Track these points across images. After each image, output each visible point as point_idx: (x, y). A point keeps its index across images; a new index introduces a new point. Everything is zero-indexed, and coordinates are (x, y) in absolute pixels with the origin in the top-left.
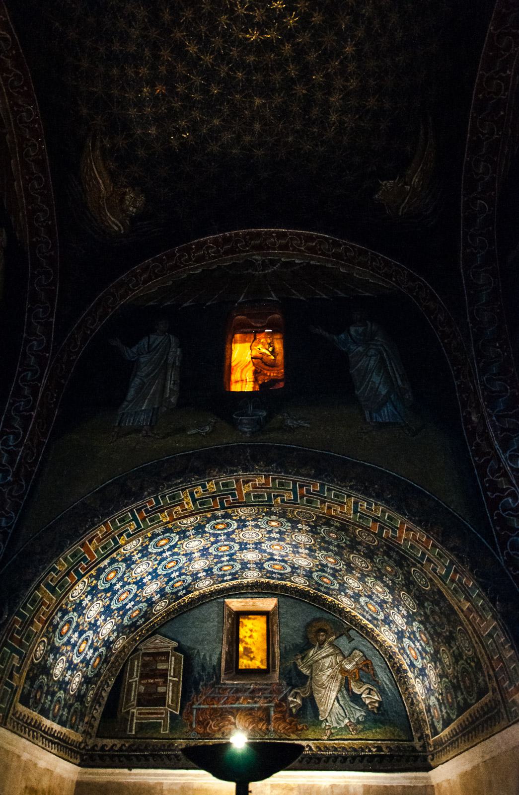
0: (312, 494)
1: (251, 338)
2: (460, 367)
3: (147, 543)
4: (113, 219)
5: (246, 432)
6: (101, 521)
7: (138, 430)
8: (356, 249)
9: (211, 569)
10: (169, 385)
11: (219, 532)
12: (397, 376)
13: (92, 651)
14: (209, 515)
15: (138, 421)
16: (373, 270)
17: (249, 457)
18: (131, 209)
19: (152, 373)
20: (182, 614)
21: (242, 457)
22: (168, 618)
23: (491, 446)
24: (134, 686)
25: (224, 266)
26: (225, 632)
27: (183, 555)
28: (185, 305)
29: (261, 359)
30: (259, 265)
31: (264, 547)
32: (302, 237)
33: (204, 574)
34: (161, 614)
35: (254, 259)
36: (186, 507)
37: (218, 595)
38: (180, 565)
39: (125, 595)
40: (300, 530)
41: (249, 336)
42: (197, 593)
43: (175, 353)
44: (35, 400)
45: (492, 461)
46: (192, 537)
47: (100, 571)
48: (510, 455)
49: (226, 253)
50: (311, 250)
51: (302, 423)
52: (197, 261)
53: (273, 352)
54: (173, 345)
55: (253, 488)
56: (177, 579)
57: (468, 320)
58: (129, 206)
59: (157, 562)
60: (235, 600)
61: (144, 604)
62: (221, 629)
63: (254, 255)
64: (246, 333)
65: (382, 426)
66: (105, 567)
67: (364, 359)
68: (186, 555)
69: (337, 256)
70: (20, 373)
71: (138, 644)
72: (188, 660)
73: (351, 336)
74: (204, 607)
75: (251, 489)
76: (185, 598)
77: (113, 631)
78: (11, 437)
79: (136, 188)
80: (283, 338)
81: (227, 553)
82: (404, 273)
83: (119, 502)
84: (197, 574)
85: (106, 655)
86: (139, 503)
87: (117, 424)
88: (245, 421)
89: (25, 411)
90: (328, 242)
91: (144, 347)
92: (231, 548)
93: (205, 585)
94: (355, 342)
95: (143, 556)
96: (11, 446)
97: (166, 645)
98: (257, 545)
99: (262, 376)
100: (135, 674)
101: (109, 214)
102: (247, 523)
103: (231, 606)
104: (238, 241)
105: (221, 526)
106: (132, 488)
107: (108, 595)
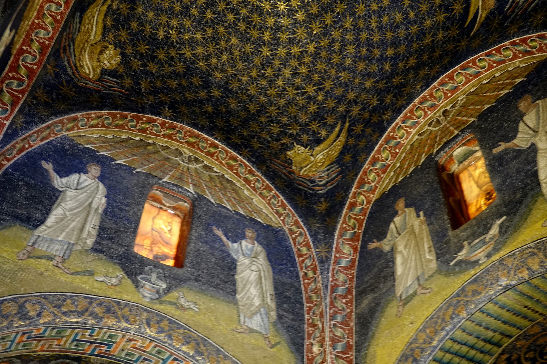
4: (88, 63)
7: (50, 258)
17: (144, 321)
18: (106, 62)
21: (138, 318)
28: (118, 162)
32: (229, 155)
43: (100, 200)
49: (164, 136)
50: (231, 167)
51: (192, 305)
52: (139, 130)
54: (100, 192)
57: (330, 274)
63: (184, 147)
67: (248, 271)
69: (248, 181)
73: (242, 248)
79: (117, 49)
83: (12, 321)
87: (30, 244)
88: (148, 287)
90: (246, 168)
94: (243, 254)
99: (157, 248)
101: (87, 57)
104: (179, 132)
106: (28, 312)
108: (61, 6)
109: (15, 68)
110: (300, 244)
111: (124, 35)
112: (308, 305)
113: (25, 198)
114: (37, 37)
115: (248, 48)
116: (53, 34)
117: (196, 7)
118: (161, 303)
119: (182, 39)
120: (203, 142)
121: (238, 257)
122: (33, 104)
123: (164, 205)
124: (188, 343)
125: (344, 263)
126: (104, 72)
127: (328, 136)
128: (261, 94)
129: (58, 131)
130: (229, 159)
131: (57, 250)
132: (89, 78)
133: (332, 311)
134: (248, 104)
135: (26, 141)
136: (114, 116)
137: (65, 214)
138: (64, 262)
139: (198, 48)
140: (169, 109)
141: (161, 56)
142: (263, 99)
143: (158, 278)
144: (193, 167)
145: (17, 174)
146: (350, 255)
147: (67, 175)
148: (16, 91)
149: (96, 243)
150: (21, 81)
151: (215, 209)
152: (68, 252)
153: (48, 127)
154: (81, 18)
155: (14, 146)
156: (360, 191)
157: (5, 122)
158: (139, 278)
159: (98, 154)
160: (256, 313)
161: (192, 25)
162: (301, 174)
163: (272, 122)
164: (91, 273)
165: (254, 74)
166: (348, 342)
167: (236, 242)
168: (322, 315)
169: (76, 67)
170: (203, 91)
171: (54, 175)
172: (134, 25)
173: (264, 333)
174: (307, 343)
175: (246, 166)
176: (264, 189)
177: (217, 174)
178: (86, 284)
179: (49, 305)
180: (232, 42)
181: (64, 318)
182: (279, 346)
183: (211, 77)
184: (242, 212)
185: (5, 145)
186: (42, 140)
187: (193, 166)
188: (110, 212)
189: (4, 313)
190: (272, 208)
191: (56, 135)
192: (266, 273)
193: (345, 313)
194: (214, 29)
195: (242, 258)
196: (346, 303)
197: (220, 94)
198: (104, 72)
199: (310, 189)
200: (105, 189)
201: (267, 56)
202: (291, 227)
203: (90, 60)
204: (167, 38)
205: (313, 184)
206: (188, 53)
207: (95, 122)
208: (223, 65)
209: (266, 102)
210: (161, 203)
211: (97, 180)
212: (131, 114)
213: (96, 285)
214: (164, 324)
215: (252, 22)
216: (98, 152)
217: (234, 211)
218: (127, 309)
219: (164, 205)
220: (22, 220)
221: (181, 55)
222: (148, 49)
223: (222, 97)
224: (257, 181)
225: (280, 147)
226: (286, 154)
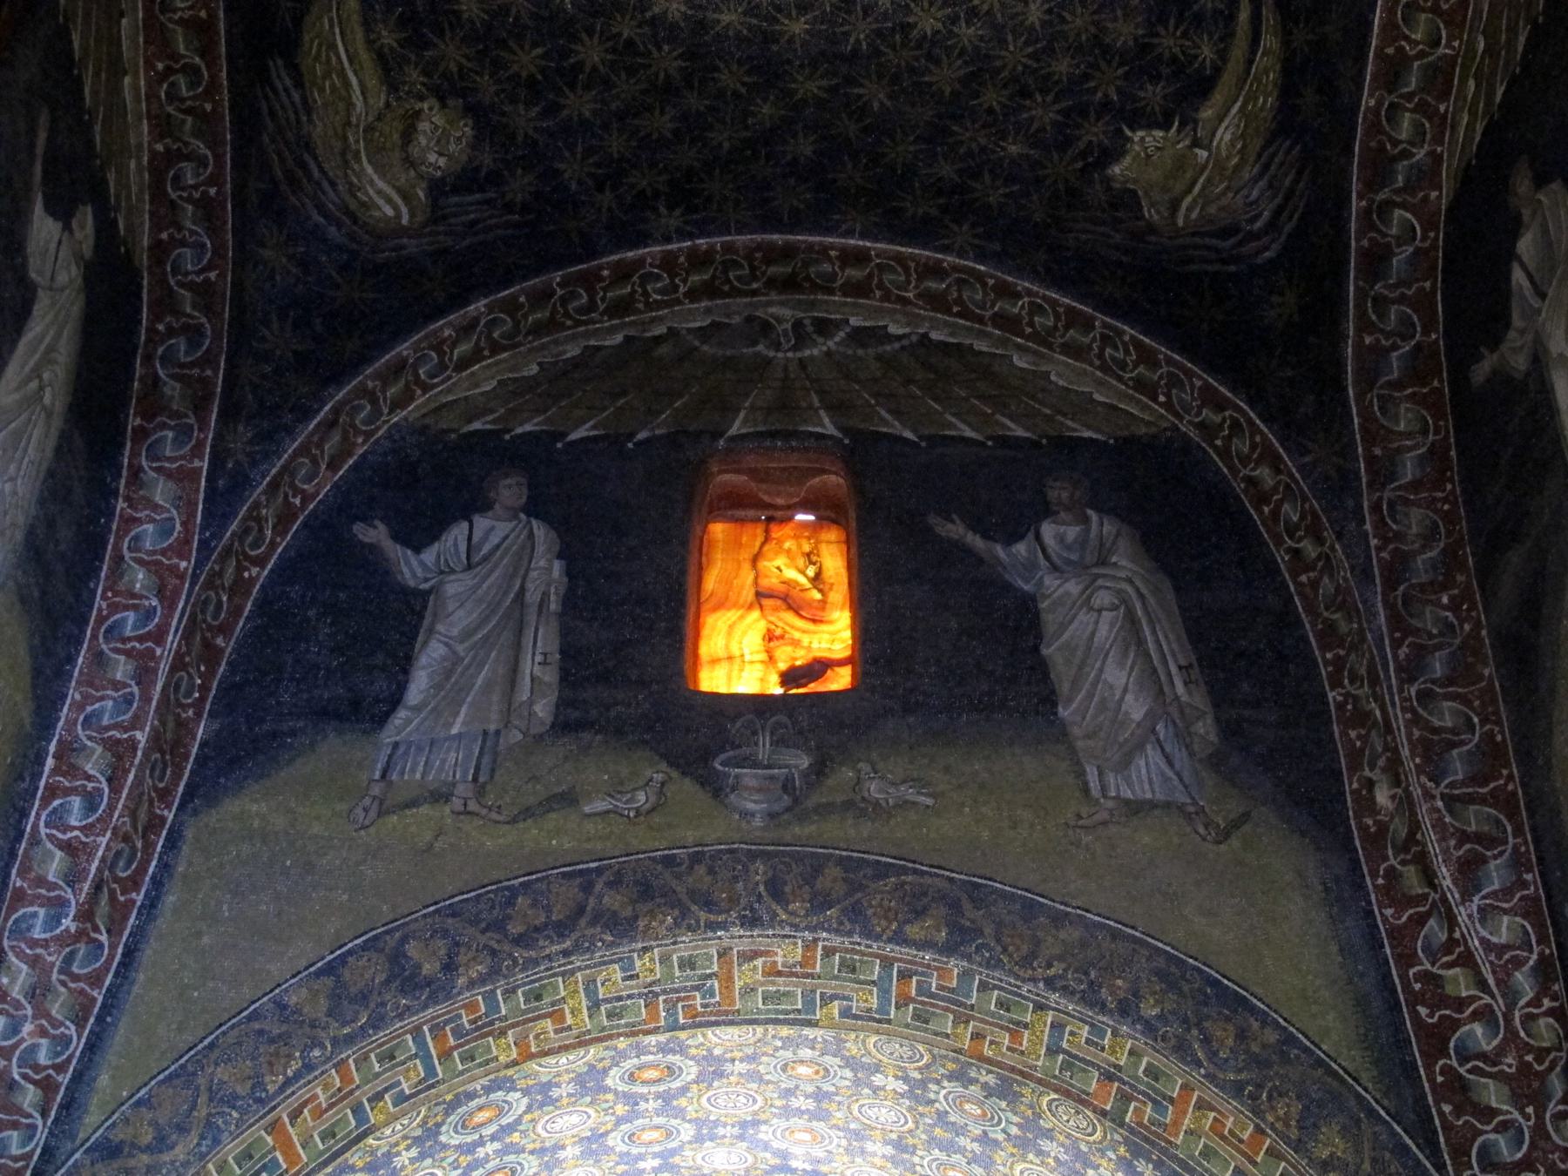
0: (932, 996)
1: (755, 536)
2: (1342, 653)
3: (439, 1119)
4: (381, 184)
5: (753, 815)
6: (329, 1059)
7: (440, 796)
8: (1061, 310)
10: (529, 666)
11: (645, 1090)
12: (1174, 670)
14: (622, 1043)
15: (441, 768)
16: (1104, 368)
17: (762, 888)
18: (432, 158)
21: (740, 885)
23: (1430, 878)
25: (689, 330)
27: (532, 1152)
28: (573, 436)
30: (785, 331)
31: (764, 1133)
35: (772, 315)
36: (569, 1021)
40: (876, 1090)
43: (547, 573)
44: (146, 699)
45: (1432, 922)
46: (565, 1101)
48: (1481, 910)
49: (693, 295)
50: (938, 302)
51: (910, 793)
53: (817, 579)
54: (540, 549)
55: (765, 974)
57: (1368, 527)
63: (769, 304)
64: (740, 521)
65: (1135, 809)
67: (1082, 616)
75: (759, 977)
78: (76, 802)
80: (848, 542)
81: (657, 1149)
82: (1192, 386)
83: (383, 1004)
86: (441, 1009)
87: (377, 775)
88: (753, 783)
90: (984, 285)
91: (457, 550)
92: (669, 1135)
94: (1055, 568)
95: (422, 1156)
96: (75, 828)
98: (747, 1127)
99: (789, 649)
101: (370, 170)
102: (728, 1067)
104: (728, 265)
105: (652, 1074)
106: (419, 966)
108: (196, 71)
109: (165, 303)
110: (1245, 461)
111: (453, 53)
112: (1329, 656)
114: (183, 189)
116: (219, 158)
118: (803, 818)
120: (817, 261)
121: (1040, 582)
122: (264, 377)
124: (920, 914)
125: (1409, 470)
126: (437, 188)
127: (1223, 55)
128: (954, 20)
131: (452, 764)
132: (403, 227)
133: (1403, 652)
136: (511, 306)
137: (454, 653)
140: (671, 208)
141: (592, 54)
142: (967, 33)
143: (779, 742)
144: (815, 352)
145: (295, 591)
146: (1425, 432)
147: (435, 538)
148: (192, 365)
149: (562, 704)
152: (486, 760)
153: (330, 424)
155: (255, 517)
156: (1381, 196)
157: (197, 463)
159: (507, 437)
160: (1141, 747)
162: (1180, 222)
163: (1025, 93)
164: (568, 799)
166: (1490, 736)
167: (1022, 537)
168: (1374, 681)
170: (765, 100)
171: (395, 552)
173: (1182, 798)
174: (1351, 785)
175: (980, 277)
176: (1067, 328)
177: (905, 342)
178: (558, 837)
179: (471, 930)
182: (1247, 828)
183: (777, 41)
184: (1020, 432)
185: (223, 527)
186: (333, 466)
188: (581, 601)
189: (353, 990)
190: (1120, 379)
192: (1152, 600)
193: (1458, 641)
195: (1050, 582)
196: (1454, 606)
197: (824, 83)
198: (437, 188)
199: (1224, 262)
200: (553, 534)
202: (1198, 414)
203: (383, 176)
205: (1232, 241)
207: (464, 348)
209: (981, 38)
211: (523, 516)
212: (558, 276)
213: (589, 827)
214: (831, 877)
216: (509, 431)
217: (989, 438)
218: (701, 870)
220: (339, 717)
222: (544, 56)
223: (832, 90)
224: (1036, 309)
225: (1080, 165)
226: (1107, 181)
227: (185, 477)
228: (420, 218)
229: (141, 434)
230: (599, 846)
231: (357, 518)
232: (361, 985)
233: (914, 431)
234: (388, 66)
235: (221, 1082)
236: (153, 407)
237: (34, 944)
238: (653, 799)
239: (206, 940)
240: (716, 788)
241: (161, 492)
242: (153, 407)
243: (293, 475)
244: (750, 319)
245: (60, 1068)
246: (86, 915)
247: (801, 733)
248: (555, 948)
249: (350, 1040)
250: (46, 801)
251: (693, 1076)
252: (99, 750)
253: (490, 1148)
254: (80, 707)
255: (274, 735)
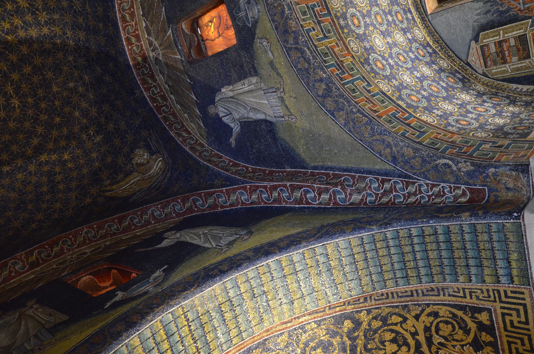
3: (381, 76)
4: (155, 167)
5: (258, 9)
7: (282, 99)
9: (403, 29)
13: (486, 104)
18: (145, 157)
19: (243, 106)
20: (447, 46)
21: (276, 5)
22: (453, 57)
24: (514, 67)
26: (454, 5)
27: (391, 50)
29: (218, 28)
33: (408, 34)
34: (451, 62)
37: (426, 21)
38: (401, 52)
39: (433, 88)
41: (207, 45)
42: (428, 39)
44: (280, 186)
47: (409, 106)
49: (155, 81)
50: (132, 15)
52: (166, 100)
53: (211, 21)
54: (221, 97)
56: (416, 54)
58: (144, 159)
59: (400, 68)
60: (427, 5)
61: (441, 75)
62: (452, 9)
63: (150, 60)
66: (407, 103)
68: (391, 48)
70: (265, 203)
71: (479, 73)
72: (483, 28)
74: (438, 29)
76: (434, 47)
77: (468, 93)
78: (308, 196)
81: (384, 17)
84: (409, 39)
85: (490, 95)
87: (283, 119)
89: (288, 191)
90: (121, 3)
92: (377, 14)
93: (420, 33)
97: (475, 50)
100: (503, 69)
101: (152, 171)
103: (433, 8)
104: (143, 73)
105: (356, 21)
106: (324, 89)
107: (433, 99)
109: (190, 210)
113: (260, 142)
115: (49, 75)
117: (61, 132)
119: (88, 122)
120: (134, 51)
122: (204, 181)
123: (198, 40)
126: (152, 153)
129: (208, 152)
130: (128, 22)
131: (274, 100)
134: (82, 40)
135: (228, 168)
136: (170, 126)
138: (278, 89)
139: (84, 107)
140: (135, 94)
141: (111, 126)
147: (229, 126)
148: (202, 199)
150: (194, 201)
151: (167, 3)
153: (209, 161)
154: (132, 196)
157: (224, 191)
158: (250, 26)
161: (75, 124)
164: (271, 63)
165: (60, 55)
169: (163, 172)
172: (109, 160)
178: (281, 62)
179: (311, 78)
180: (57, 89)
181: (312, 61)
185: (238, 180)
186: (221, 157)
187: (156, 43)
191: (212, 151)
194: (62, 109)
197: (96, 66)
201: (40, 56)
204: (97, 133)
206: (94, 111)
207: (184, 134)
208: (77, 82)
209: (69, 29)
210: (199, 44)
213: (276, 55)
215: (30, 88)
219: (198, 40)
221: (99, 114)
227: (228, 193)
228: (160, 156)
229: (222, 207)
230: (279, 50)
231: (231, 147)
232: (333, 104)
233: (162, 8)
234: (127, 174)
235: (369, 134)
236: (215, 206)
237: (346, 196)
238: (264, 40)
239: (336, 151)
240: (256, 23)
241: (233, 198)
242: (215, 206)
243: (223, 167)
244: (156, 64)
245: (378, 179)
246: (336, 185)
247: (235, 5)
248: (308, 52)
249: (348, 102)
250: (310, 204)
251: (354, 10)
252: (294, 194)
253: (390, 61)
254: (286, 202)
255: (284, 150)
